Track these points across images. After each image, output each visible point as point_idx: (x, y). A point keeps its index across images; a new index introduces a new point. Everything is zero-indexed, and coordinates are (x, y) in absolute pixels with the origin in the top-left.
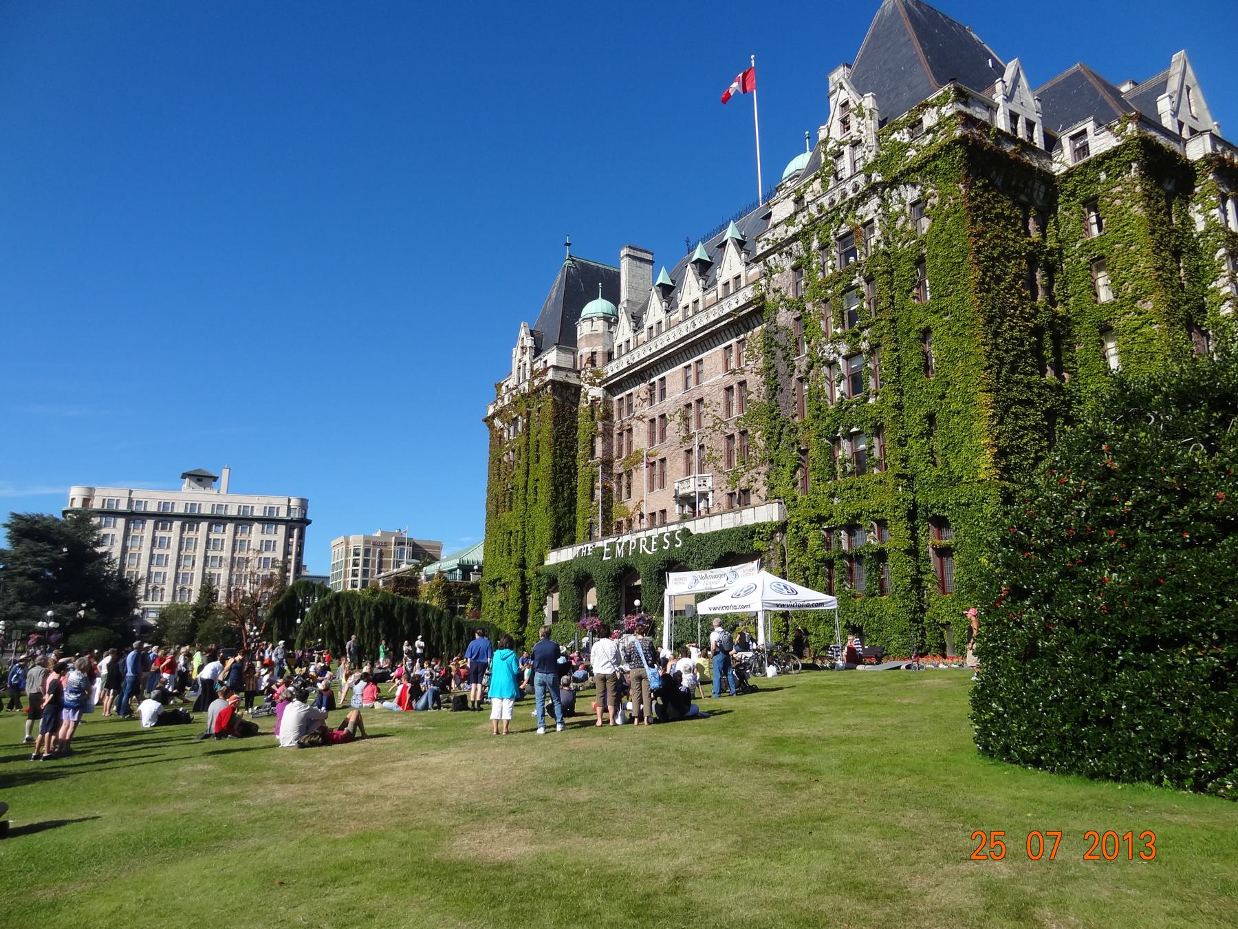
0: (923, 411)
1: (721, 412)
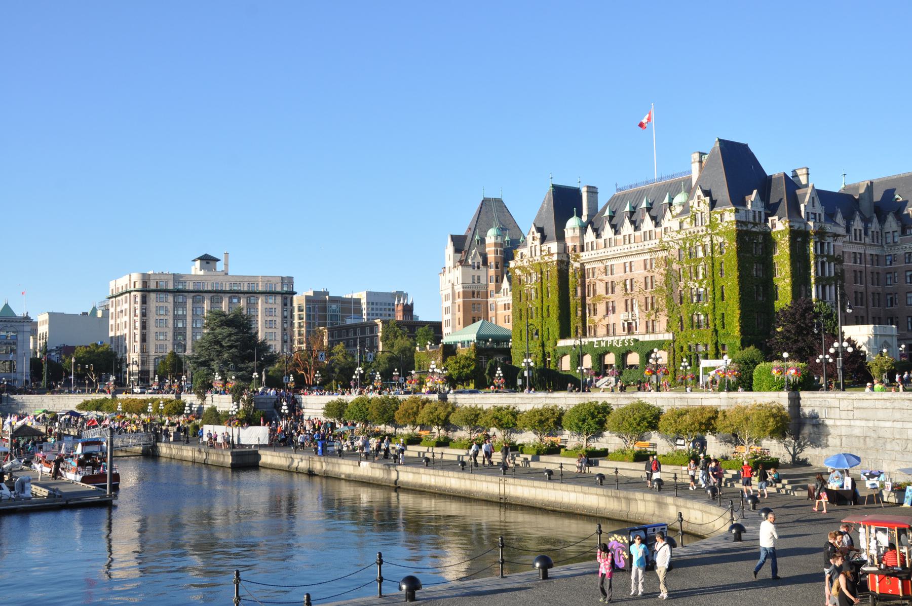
0: (721, 312)
1: (643, 286)
